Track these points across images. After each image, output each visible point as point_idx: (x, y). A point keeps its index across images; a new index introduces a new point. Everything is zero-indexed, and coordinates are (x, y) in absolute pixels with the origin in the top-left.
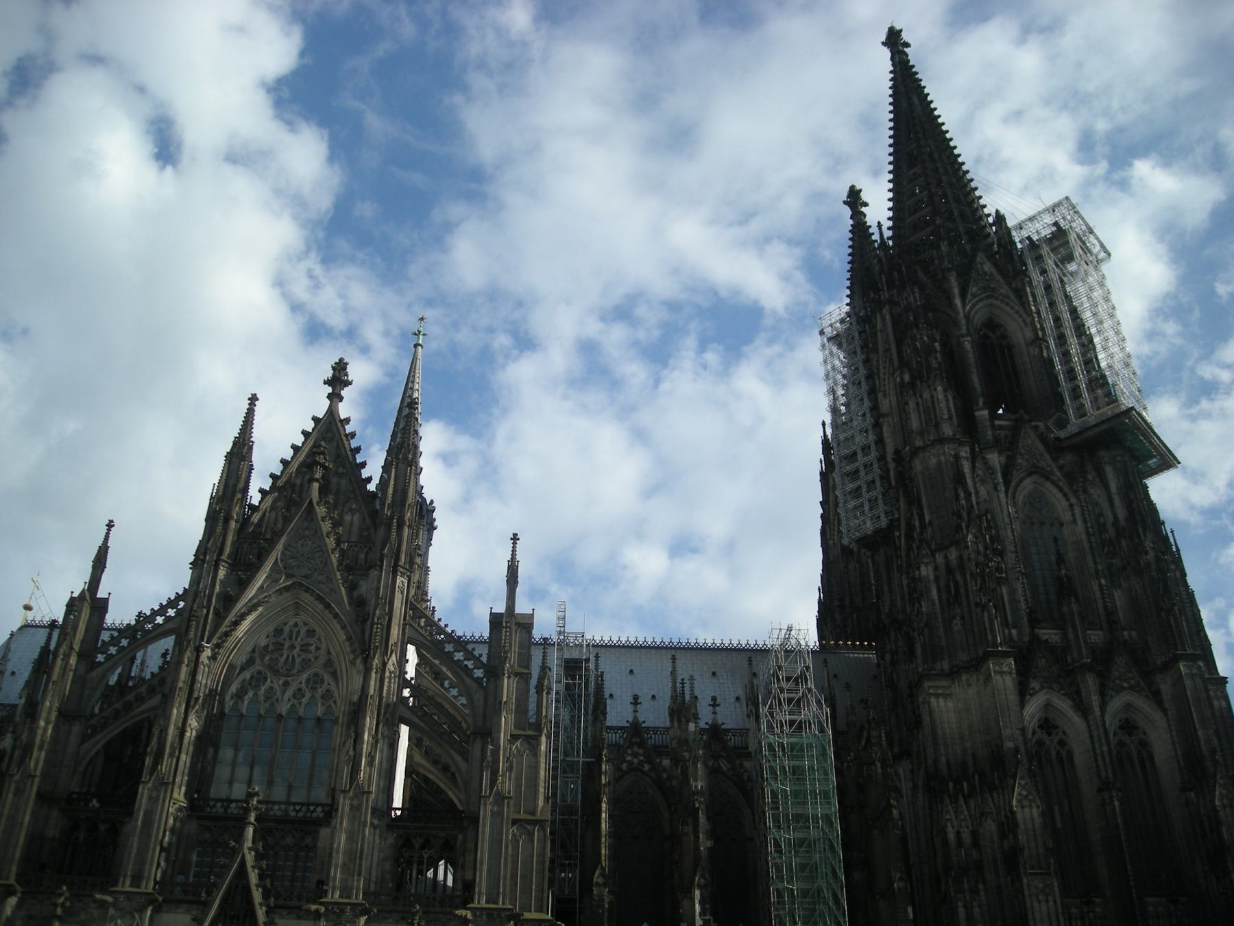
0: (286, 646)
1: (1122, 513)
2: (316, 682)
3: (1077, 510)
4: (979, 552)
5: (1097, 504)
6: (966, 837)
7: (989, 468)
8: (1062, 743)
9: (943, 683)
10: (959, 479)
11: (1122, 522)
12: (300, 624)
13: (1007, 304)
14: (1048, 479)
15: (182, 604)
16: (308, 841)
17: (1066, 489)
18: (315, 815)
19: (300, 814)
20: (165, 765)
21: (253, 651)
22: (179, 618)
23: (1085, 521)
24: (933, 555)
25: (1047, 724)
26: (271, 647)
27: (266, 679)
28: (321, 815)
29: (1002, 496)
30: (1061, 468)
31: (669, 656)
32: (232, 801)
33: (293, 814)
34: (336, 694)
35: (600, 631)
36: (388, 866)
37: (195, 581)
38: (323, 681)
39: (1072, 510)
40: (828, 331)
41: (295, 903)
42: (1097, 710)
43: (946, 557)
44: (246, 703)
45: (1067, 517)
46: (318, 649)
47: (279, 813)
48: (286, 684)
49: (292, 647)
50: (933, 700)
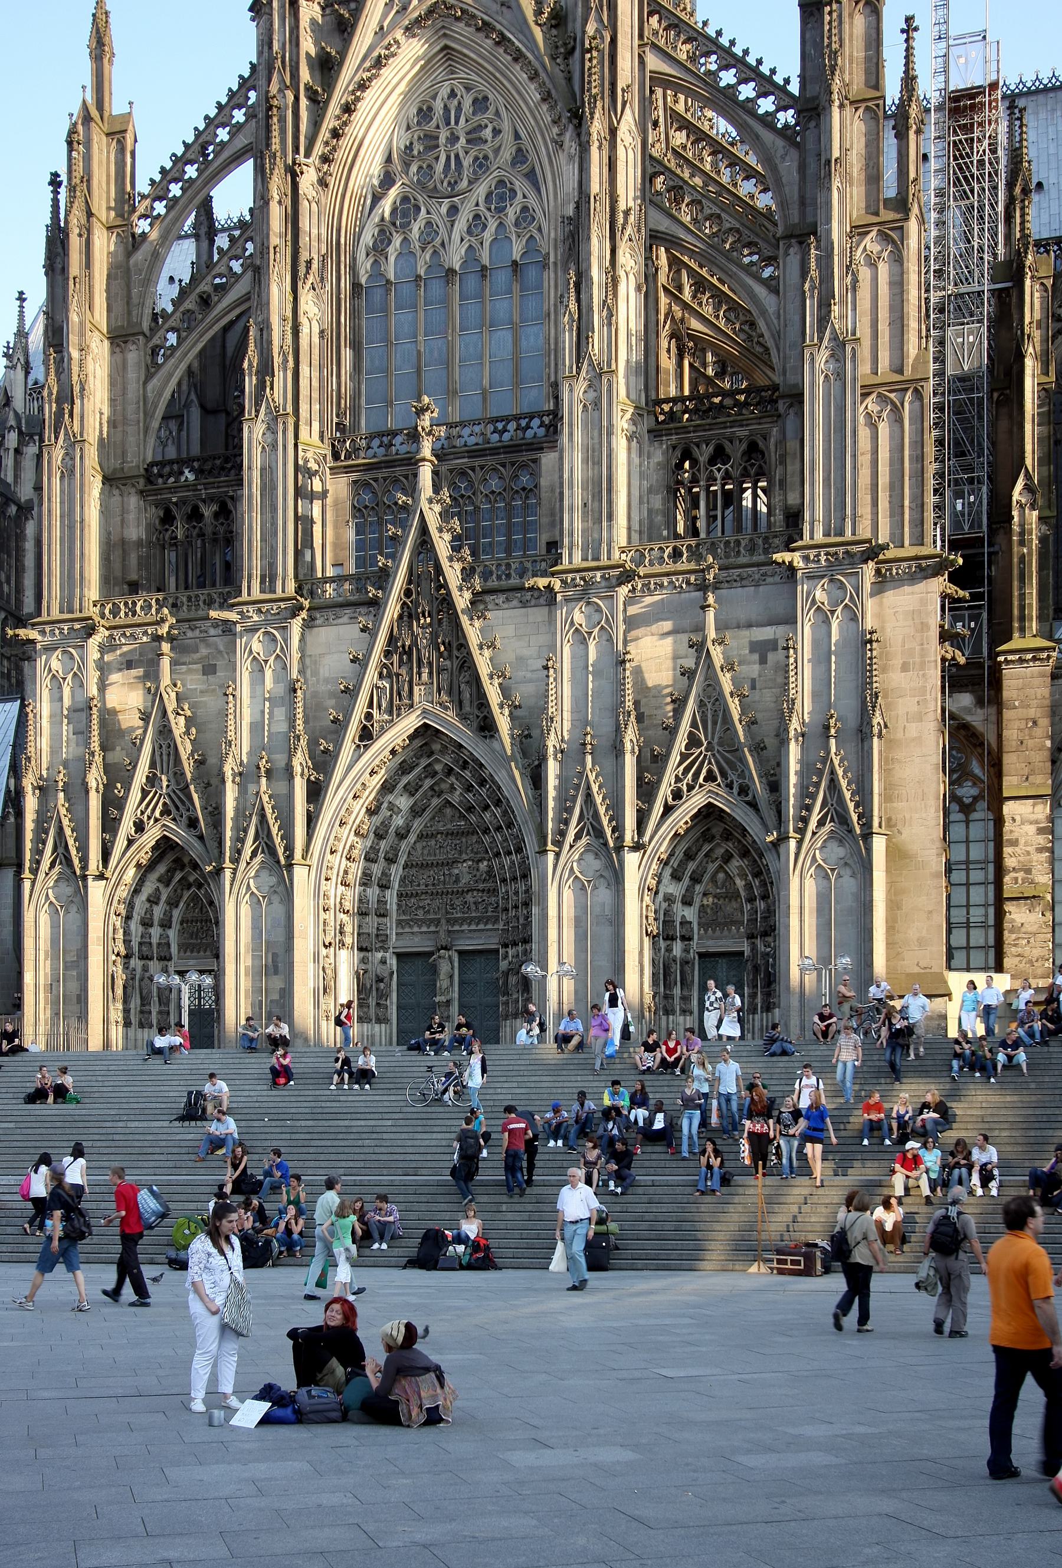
0: (442, 140)
2: (502, 198)
12: (460, 90)
15: (252, 95)
16: (525, 479)
18: (529, 433)
19: (506, 436)
20: (279, 389)
21: (389, 160)
22: (253, 123)
26: (417, 148)
27: (418, 209)
28: (542, 432)
32: (394, 434)
33: (496, 437)
34: (539, 214)
36: (657, 502)
37: (265, 42)
38: (513, 192)
41: (514, 581)
44: (392, 259)
46: (496, 132)
47: (472, 440)
48: (454, 210)
49: (453, 139)
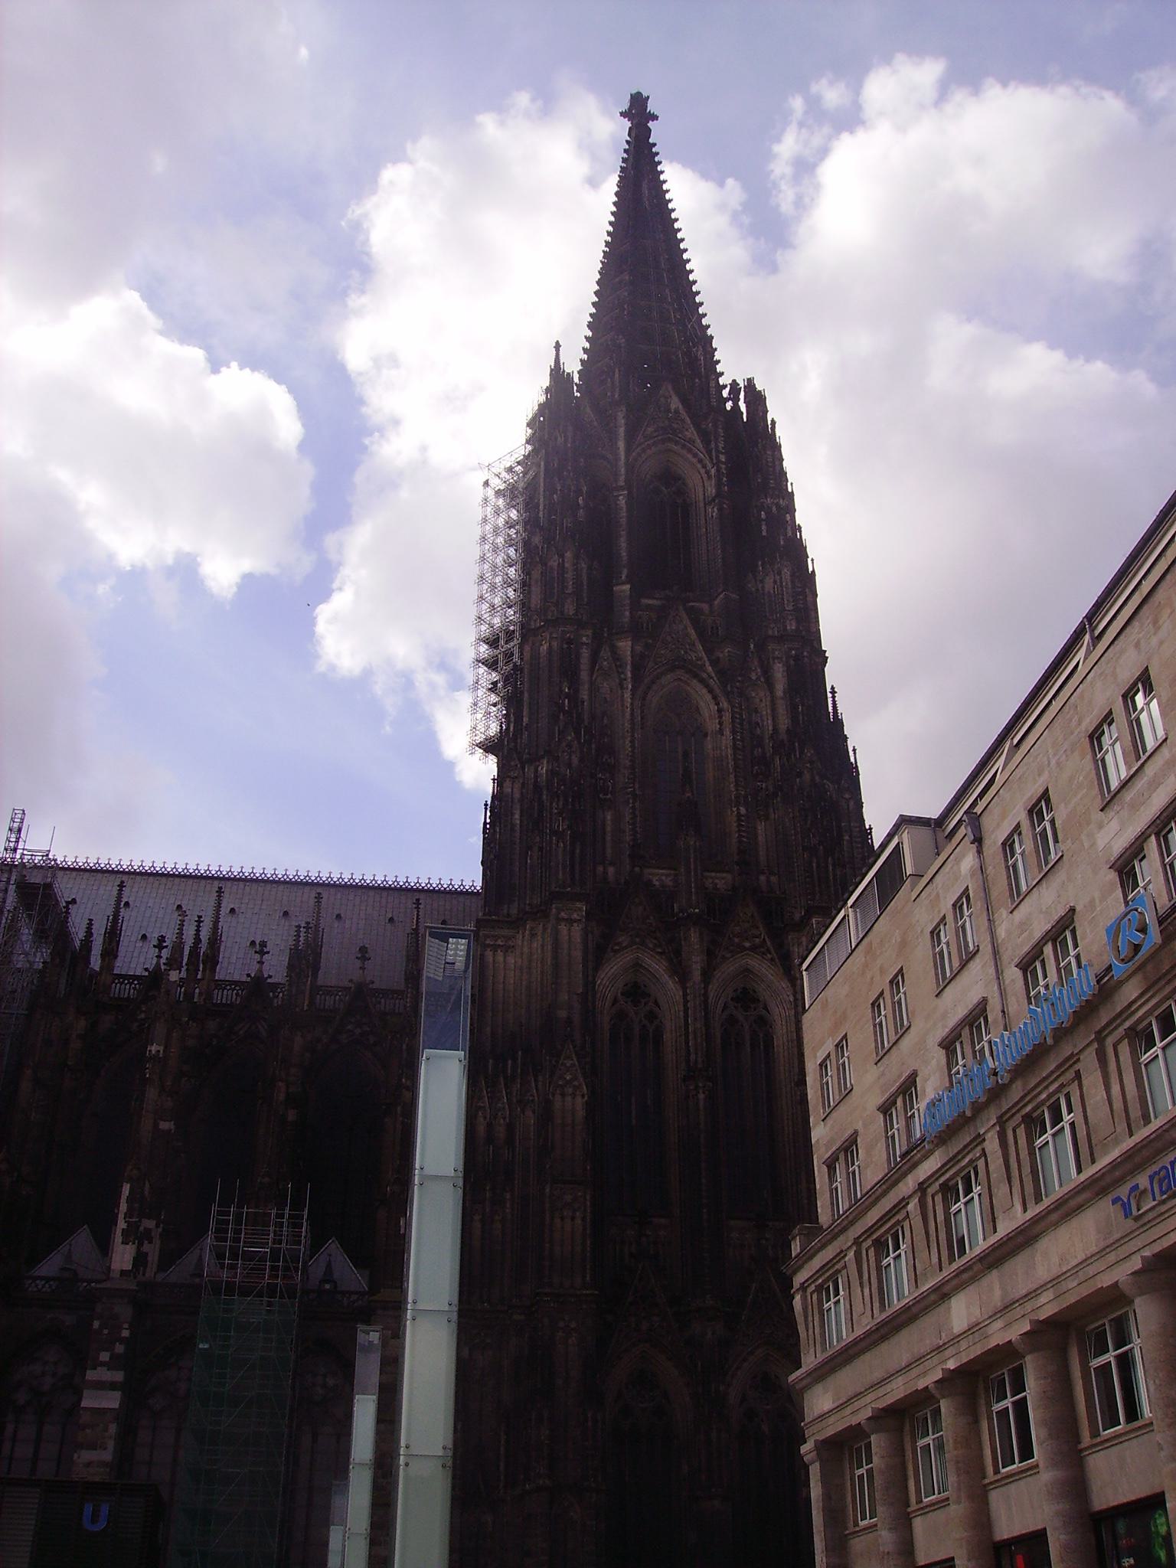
1: (784, 722)
3: (727, 717)
4: (569, 765)
5: (756, 711)
6: (501, 1132)
7: (616, 657)
8: (652, 1016)
9: (506, 932)
10: (570, 672)
11: (783, 736)
13: (690, 451)
14: (696, 676)
17: (718, 691)
23: (734, 732)
24: (523, 768)
25: (636, 992)
29: (628, 695)
30: (714, 663)
31: (313, 895)
35: (68, 851)
39: (720, 717)
40: (497, 484)
42: (697, 975)
43: (536, 771)
45: (712, 725)
50: (489, 953)
